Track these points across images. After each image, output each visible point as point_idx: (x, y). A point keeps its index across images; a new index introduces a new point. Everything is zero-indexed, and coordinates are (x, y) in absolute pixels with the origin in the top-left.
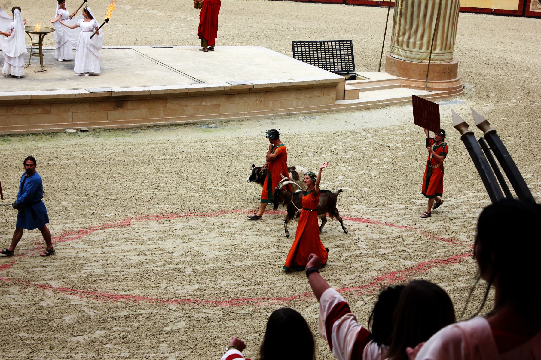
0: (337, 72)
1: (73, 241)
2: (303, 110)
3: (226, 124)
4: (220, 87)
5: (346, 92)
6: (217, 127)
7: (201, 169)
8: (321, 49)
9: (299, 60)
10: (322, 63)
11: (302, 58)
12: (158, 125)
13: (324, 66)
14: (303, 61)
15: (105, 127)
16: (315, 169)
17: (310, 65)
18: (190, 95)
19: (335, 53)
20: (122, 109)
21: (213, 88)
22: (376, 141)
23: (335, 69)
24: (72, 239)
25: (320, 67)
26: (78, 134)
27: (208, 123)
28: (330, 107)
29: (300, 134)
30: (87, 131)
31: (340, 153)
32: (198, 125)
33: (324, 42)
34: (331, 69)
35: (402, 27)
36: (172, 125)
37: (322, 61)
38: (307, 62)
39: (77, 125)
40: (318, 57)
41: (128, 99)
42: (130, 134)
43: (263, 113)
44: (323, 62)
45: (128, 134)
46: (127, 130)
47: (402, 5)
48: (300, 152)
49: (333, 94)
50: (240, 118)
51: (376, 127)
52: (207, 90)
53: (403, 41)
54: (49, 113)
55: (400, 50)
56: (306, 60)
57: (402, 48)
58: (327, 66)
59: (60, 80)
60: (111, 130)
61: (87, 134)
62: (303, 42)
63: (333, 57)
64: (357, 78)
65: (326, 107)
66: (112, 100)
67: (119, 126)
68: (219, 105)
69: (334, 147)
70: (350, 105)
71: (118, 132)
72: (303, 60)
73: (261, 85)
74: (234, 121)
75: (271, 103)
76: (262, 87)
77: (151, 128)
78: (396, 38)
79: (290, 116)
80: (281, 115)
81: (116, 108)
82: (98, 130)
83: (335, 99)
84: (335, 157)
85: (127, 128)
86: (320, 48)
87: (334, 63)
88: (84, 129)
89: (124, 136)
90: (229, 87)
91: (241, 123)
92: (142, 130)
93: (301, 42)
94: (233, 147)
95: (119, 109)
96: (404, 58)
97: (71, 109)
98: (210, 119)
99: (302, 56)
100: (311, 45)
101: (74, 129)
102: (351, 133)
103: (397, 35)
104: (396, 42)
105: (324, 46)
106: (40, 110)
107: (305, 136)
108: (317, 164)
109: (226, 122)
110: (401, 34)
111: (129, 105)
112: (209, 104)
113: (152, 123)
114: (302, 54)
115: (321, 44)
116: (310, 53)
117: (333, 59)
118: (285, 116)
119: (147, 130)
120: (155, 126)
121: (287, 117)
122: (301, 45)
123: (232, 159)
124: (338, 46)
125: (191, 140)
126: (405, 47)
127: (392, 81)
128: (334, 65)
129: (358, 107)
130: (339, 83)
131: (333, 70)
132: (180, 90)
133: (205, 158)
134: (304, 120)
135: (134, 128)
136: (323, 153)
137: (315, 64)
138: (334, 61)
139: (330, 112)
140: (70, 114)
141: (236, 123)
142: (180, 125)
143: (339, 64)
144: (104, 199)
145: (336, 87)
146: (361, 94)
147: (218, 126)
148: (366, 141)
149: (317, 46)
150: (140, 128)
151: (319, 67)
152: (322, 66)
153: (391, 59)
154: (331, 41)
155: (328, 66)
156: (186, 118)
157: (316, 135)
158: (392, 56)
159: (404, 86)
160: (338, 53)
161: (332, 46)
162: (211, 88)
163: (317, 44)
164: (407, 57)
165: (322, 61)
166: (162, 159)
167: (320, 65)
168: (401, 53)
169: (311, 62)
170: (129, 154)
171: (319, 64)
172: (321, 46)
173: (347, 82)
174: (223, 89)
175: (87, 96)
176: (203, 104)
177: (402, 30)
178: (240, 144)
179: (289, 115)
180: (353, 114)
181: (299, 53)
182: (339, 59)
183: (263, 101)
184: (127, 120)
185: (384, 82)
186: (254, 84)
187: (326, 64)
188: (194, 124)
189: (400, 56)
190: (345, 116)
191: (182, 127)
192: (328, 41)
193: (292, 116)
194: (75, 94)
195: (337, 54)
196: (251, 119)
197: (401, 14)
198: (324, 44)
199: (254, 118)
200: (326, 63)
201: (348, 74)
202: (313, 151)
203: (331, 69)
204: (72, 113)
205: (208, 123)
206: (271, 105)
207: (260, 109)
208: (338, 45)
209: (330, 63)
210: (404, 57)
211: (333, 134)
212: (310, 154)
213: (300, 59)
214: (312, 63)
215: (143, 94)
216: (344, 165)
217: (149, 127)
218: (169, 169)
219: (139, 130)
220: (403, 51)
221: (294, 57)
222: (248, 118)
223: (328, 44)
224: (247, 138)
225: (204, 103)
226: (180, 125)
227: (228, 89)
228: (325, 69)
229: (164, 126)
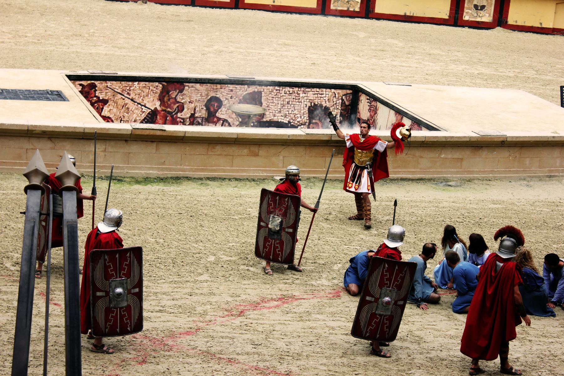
1: (271, 310)
3: (469, 182)
4: (465, 137)
6: (457, 186)
7: (433, 235)
15: (321, 176)
18: (427, 144)
21: (456, 137)
24: (269, 308)
27: (446, 180)
29: (561, 201)
32: (434, 181)
36: (402, 179)
43: (517, 172)
48: (560, 224)
52: (448, 140)
54: (256, 155)
66: (332, 145)
67: (337, 177)
68: (462, 159)
73: (517, 137)
74: (479, 179)
75: (527, 161)
76: (518, 140)
79: (551, 178)
80: (539, 177)
81: (336, 154)
82: (312, 180)
90: (475, 137)
91: (488, 182)
94: (474, 211)
97: (282, 153)
98: (449, 175)
106: (245, 151)
109: (470, 180)
112: (450, 156)
118: (545, 178)
121: (548, 179)
123: (473, 226)
125: (423, 199)
133: (439, 223)
140: (281, 158)
141: (481, 182)
142: (412, 180)
144: (312, 263)
147: (459, 184)
156: (420, 173)
162: (453, 137)
166: (385, 219)
170: (347, 211)
174: (468, 140)
175: (302, 138)
176: (443, 156)
178: (484, 209)
179: (550, 177)
186: (508, 136)
188: (430, 180)
191: (414, 183)
193: (554, 179)
194: (288, 134)
196: (501, 179)
199: (505, 177)
204: (284, 157)
205: (446, 180)
206: (527, 162)
207: (514, 168)
222: (497, 177)
224: (494, 202)
225: (443, 155)
226: (412, 180)
227: (474, 140)
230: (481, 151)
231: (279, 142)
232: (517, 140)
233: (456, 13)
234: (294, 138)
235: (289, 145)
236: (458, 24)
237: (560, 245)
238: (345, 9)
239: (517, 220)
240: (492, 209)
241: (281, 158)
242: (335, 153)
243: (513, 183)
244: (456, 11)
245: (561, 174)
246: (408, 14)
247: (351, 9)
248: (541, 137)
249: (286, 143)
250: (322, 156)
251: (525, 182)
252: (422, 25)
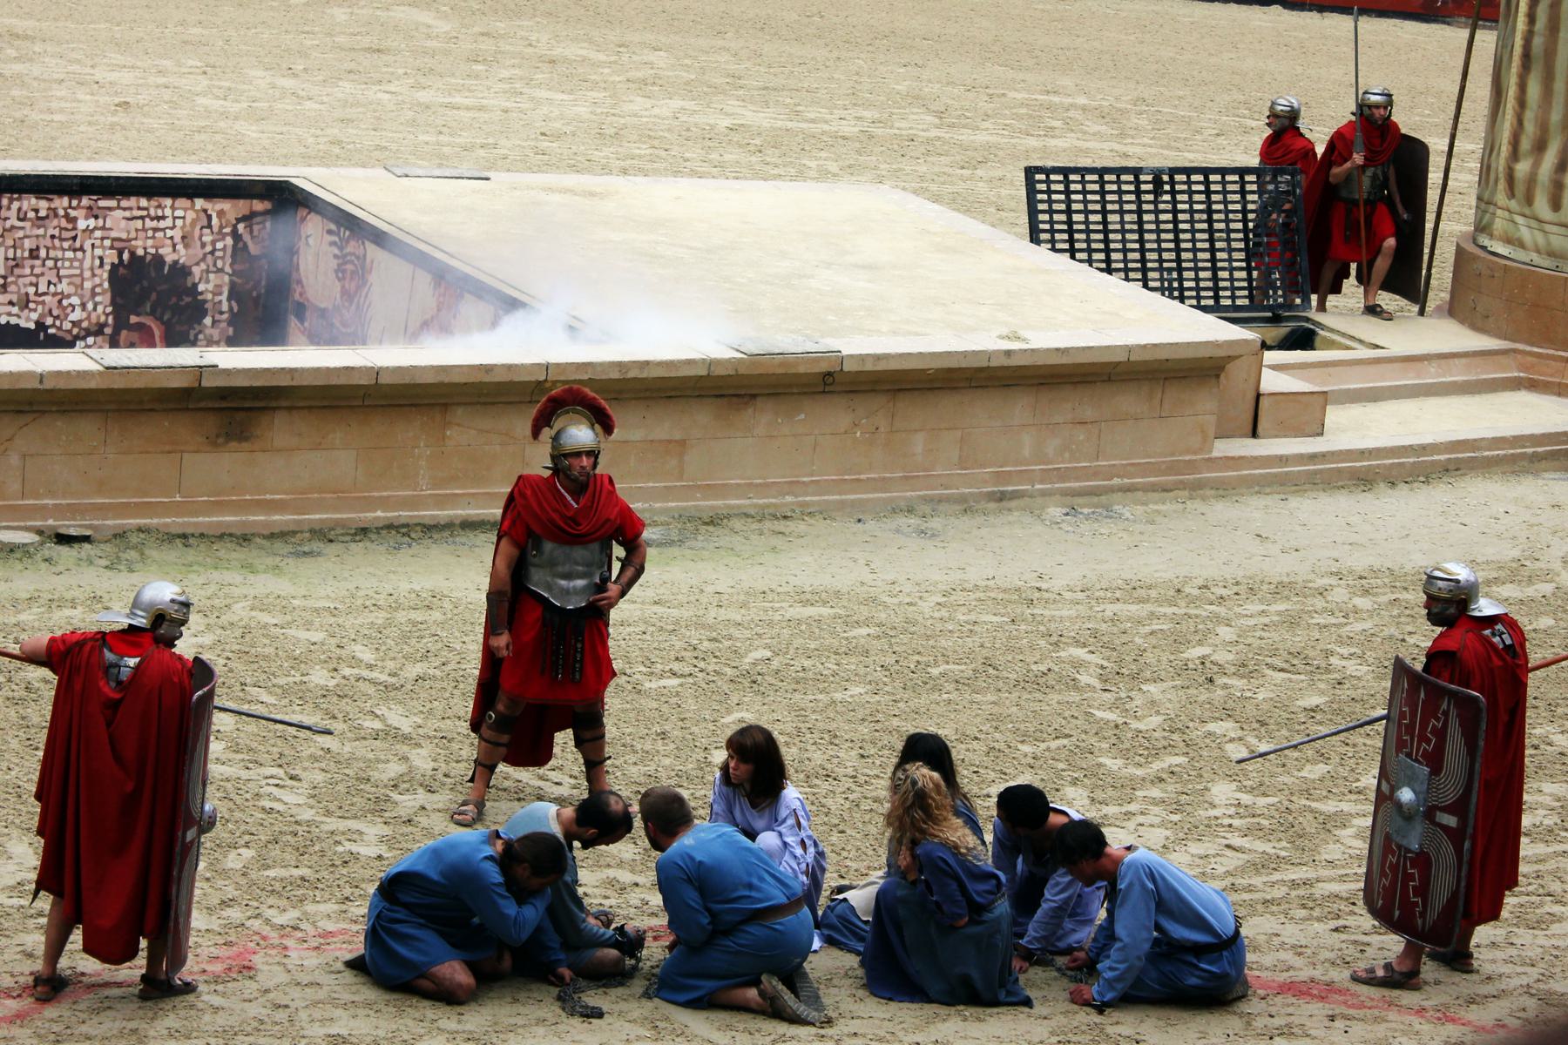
0: (1226, 309)
2: (1063, 475)
3: (711, 528)
4: (690, 362)
5: (1264, 403)
6: (671, 543)
8: (1155, 202)
9: (1054, 249)
10: (1161, 269)
11: (1071, 241)
12: (404, 526)
13: (1170, 281)
14: (1073, 257)
15: (166, 525)
16: (1105, 745)
17: (1105, 275)
19: (1222, 226)
20: (245, 445)
21: (660, 364)
22: (1393, 630)
23: (1217, 298)
25: (1151, 284)
26: (47, 553)
28: (1191, 466)
29: (1044, 586)
30: (86, 539)
31: (1225, 680)
33: (1173, 171)
34: (1198, 298)
35: (1529, 116)
37: (1161, 261)
38: (1090, 262)
39: (43, 511)
40: (1141, 241)
41: (274, 404)
42: (279, 559)
43: (883, 484)
44: (1165, 265)
45: (270, 561)
46: (264, 542)
47: (1531, 18)
48: (1043, 668)
49: (1204, 405)
50: (775, 505)
51: (1396, 568)
52: (631, 375)
53: (1532, 181)
55: (1519, 219)
56: (1090, 251)
57: (1527, 211)
58: (1181, 279)
60: (191, 541)
61: (83, 555)
62: (1076, 170)
63: (1211, 240)
64: (1318, 341)
65: (1172, 468)
66: (202, 405)
67: (229, 524)
68: (682, 443)
69: (1196, 652)
70: (1283, 460)
71: (224, 551)
72: (1072, 252)
73: (878, 358)
74: (747, 515)
75: (919, 443)
76: (881, 367)
77: (373, 536)
78: (1501, 163)
79: (1005, 504)
80: (962, 499)
81: (221, 440)
82: (134, 539)
83: (1211, 434)
84: (1202, 698)
85: (266, 532)
86: (1151, 197)
87: (1214, 270)
88: (73, 532)
89: (250, 568)
90: (729, 361)
91: (780, 526)
92: (333, 545)
93: (1066, 171)
95: (233, 444)
96: (1535, 257)
99: (1071, 232)
100: (1114, 187)
101: (27, 529)
102: (1281, 589)
103: (1505, 149)
104: (1502, 185)
105: (1173, 192)
107: (1068, 595)
108: (1117, 726)
110: (1525, 144)
111: (281, 430)
113: (379, 513)
114: (1070, 222)
115: (1157, 182)
116: (1105, 222)
117: (1213, 250)
118: (983, 505)
119: (353, 546)
120: (390, 527)
121: (992, 505)
122: (1067, 182)
124: (1234, 192)
126: (1541, 205)
127: (1478, 360)
128: (1215, 279)
129: (1316, 472)
130: (1230, 359)
131: (1211, 302)
132: (509, 367)
134: (1070, 524)
135: (294, 533)
136: (1148, 674)
137: (1126, 270)
138: (1213, 260)
139: (1186, 493)
140: (14, 460)
141: (755, 526)
143: (1237, 274)
145: (1218, 376)
146: (1335, 416)
147: (674, 535)
148: (1348, 628)
149: (1138, 192)
150: (323, 534)
151: (1146, 286)
152: (1162, 280)
153: (1475, 258)
154: (1206, 172)
155: (1186, 284)
157: (1118, 594)
158: (1484, 248)
159: (1533, 385)
160: (1233, 226)
161: (1208, 192)
162: (647, 363)
163: (1138, 182)
164: (1551, 254)
165: (1161, 261)
167: (1151, 275)
168: (1525, 234)
169: (1108, 261)
170: (267, 650)
171: (1144, 270)
172: (1157, 191)
173: (1271, 357)
174: (703, 372)
175: (93, 385)
177: (1530, 127)
178: (771, 624)
179: (1001, 497)
180: (1294, 502)
181: (1056, 217)
182: (1240, 250)
183: (882, 429)
184: (268, 497)
185: (1443, 362)
186: (847, 351)
187: (1180, 275)
189: (1521, 245)
190: (1255, 511)
192: (1188, 171)
193: (1013, 504)
194: (39, 370)
195: (1229, 231)
196: (825, 512)
197: (1527, 56)
198: (1172, 182)
200: (1180, 270)
201: (1276, 320)
202: (1102, 667)
203: (1198, 298)
206: (919, 449)
208: (1236, 187)
209: (1196, 269)
210: (1538, 251)
211: (1196, 592)
212: (1084, 679)
213: (1059, 246)
214: (1114, 265)
215: (342, 381)
216: (1240, 733)
217: (362, 532)
218: (442, 724)
219: (316, 546)
220: (1534, 223)
221: (1034, 238)
223: (1189, 183)
227: (723, 372)
228: (1171, 297)
229: (431, 529)
230: (750, 411)
232: (879, 368)
234: (62, 385)
235: (43, 412)
237: (1043, 746)
239: (890, 659)
240: (799, 621)
241: (14, 460)
242: (218, 436)
243: (871, 525)
245: (1038, 486)
248: (965, 354)
249: (31, 404)
250: (168, 448)
251: (913, 521)
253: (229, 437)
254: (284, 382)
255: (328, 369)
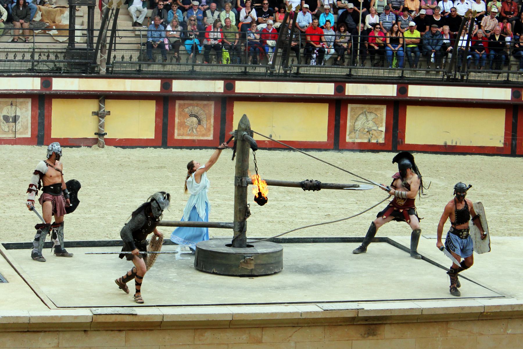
18: (486, 316)
20: (375, 337)
41: (385, 322)
52: (515, 310)
59: (278, 288)
66: (359, 323)
81: (366, 336)
95: (371, 337)
106: (244, 337)
111: (387, 331)
140: (292, 344)
176: (509, 332)
194: (300, 311)
204: (296, 342)
215: (409, 313)
231: (289, 323)
233: (513, 139)
234: (308, 316)
235: (302, 327)
236: (517, 153)
238: (366, 141)
241: (292, 344)
242: (365, 334)
244: (513, 136)
246: (449, 143)
247: (374, 141)
249: (298, 323)
252: (468, 157)
253: (369, 334)
254: (389, 314)
255: (404, 309)
